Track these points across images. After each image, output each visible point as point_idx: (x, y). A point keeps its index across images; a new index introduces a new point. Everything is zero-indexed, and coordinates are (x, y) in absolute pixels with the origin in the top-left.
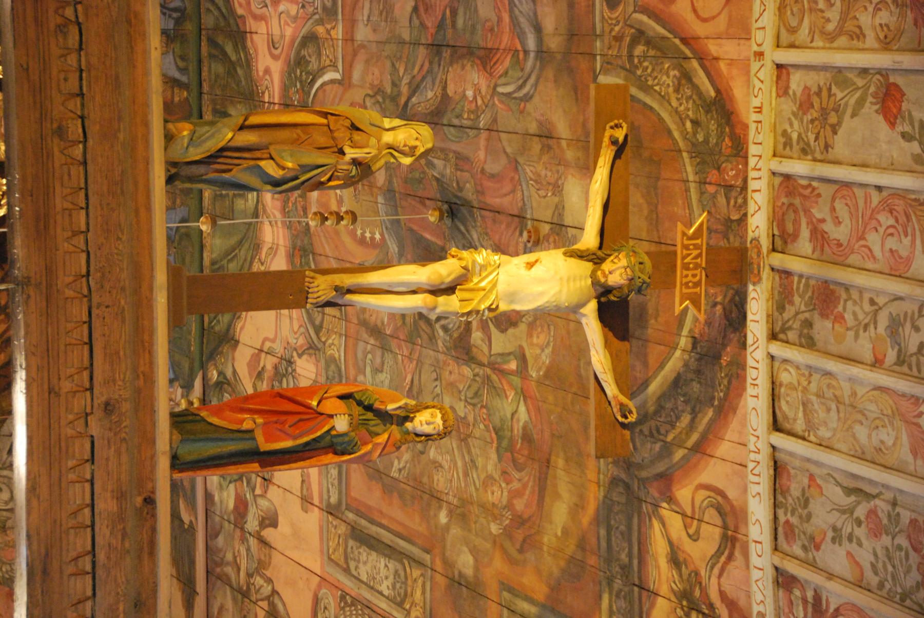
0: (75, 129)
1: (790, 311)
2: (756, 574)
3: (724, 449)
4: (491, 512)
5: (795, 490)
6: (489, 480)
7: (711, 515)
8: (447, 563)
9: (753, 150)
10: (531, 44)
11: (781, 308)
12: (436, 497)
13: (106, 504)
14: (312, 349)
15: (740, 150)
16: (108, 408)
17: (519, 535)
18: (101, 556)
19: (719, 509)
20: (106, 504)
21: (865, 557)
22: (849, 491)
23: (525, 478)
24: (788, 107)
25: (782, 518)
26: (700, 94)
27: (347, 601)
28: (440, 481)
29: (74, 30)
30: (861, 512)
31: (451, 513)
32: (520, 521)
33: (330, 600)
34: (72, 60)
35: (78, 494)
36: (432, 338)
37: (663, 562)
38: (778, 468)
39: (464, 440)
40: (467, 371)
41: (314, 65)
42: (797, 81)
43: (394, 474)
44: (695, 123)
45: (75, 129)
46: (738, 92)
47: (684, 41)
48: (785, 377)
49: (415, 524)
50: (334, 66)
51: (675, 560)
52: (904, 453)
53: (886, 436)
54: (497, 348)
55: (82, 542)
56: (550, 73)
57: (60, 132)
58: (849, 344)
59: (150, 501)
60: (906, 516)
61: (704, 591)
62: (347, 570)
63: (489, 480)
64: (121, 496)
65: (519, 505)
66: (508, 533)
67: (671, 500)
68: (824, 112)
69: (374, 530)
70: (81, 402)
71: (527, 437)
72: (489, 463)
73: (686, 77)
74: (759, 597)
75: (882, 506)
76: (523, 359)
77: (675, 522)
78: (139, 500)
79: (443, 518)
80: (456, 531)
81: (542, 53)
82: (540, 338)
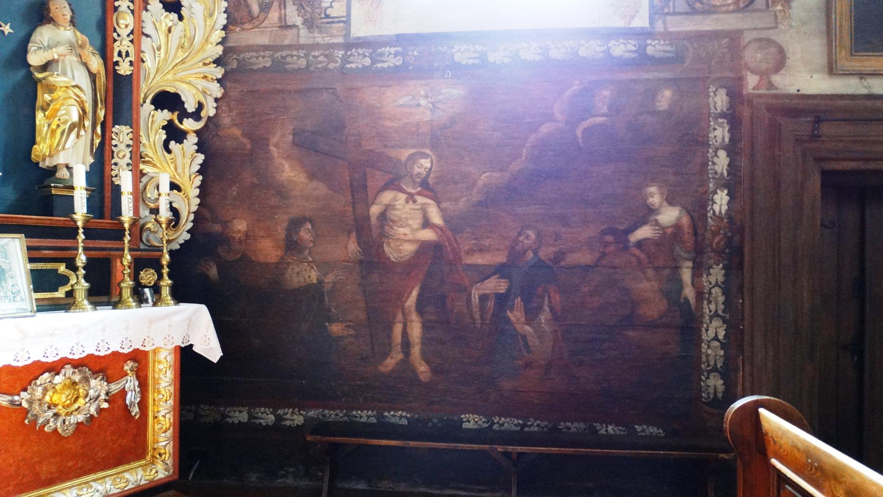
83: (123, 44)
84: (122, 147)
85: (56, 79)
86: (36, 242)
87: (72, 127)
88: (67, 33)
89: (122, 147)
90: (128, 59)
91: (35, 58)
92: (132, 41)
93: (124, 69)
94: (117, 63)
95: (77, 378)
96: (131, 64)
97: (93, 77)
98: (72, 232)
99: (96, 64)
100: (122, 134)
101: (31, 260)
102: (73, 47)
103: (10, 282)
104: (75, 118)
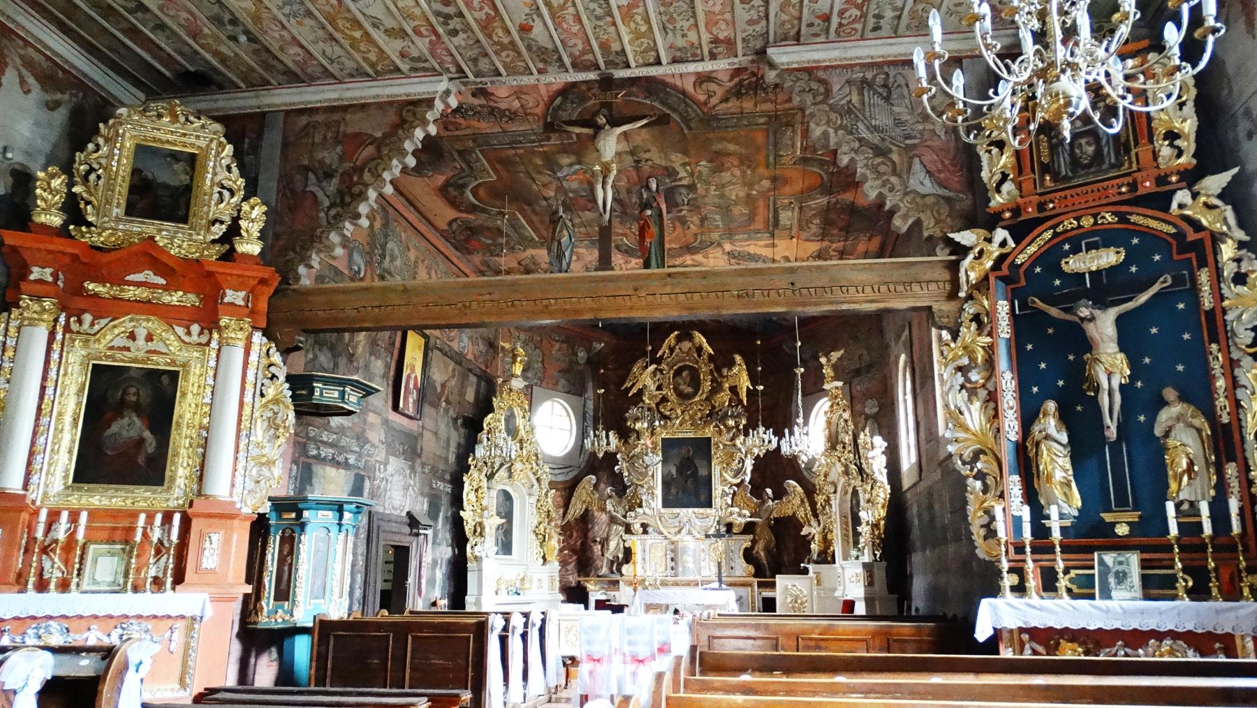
0: (545, 302)
1: (617, 61)
2: (715, 68)
3: (679, 83)
4: (744, 173)
5: (678, 54)
6: (732, 175)
7: (704, 86)
8: (770, 190)
9: (569, 80)
10: (577, 167)
11: (617, 64)
12: (748, 195)
13: (668, 289)
14: (720, 245)
15: (574, 85)
16: (636, 289)
17: (748, 163)
18: (686, 290)
19: (701, 84)
20: (668, 289)
21: (686, 24)
22: (667, 33)
23: (725, 159)
24: (550, 69)
25: (691, 59)
26: (562, 103)
27: (801, 228)
28: (742, 194)
29: (517, 303)
30: (671, 27)
31: (752, 190)
32: (742, 163)
33: (804, 235)
34: (525, 303)
35: (665, 299)
36: (695, 199)
37: (730, 104)
38: (675, 61)
39: (723, 186)
40: (699, 185)
41: (625, 247)
42: (541, 65)
43: (747, 212)
44: (573, 103)
45: (545, 302)
46: (555, 88)
47: (548, 109)
48: (641, 61)
49: (761, 203)
50: (622, 240)
51: (725, 100)
52: (640, 10)
53: (638, 18)
54: (685, 175)
55: (682, 297)
56: (583, 159)
57: (546, 307)
58: (614, 35)
59: (669, 275)
60: (662, 9)
61: (731, 88)
62: (791, 228)
63: (732, 175)
64: (665, 285)
65: (736, 163)
66: (749, 167)
67: (706, 103)
68: (543, 53)
69: (771, 220)
70: (634, 299)
71: (711, 161)
72: (726, 176)
73: (559, 107)
74: (722, 66)
75: (664, 18)
76: (684, 165)
77: (714, 101)
78: (669, 279)
79: (754, 192)
80: (757, 187)
81: (579, 163)
82: (673, 158)
83: (1221, 401)
84: (1233, 479)
85: (1171, 442)
86: (1146, 556)
87: (1184, 472)
88: (1176, 409)
89: (1233, 479)
90: (1225, 412)
91: (1158, 431)
92: (1226, 397)
93: (1225, 419)
94: (1220, 416)
95: (1174, 647)
96: (1229, 414)
97: (1199, 431)
98: (1169, 548)
99: (1200, 421)
100: (1231, 470)
101: (1143, 568)
102: (1179, 418)
103: (1129, 580)
104: (1185, 466)
